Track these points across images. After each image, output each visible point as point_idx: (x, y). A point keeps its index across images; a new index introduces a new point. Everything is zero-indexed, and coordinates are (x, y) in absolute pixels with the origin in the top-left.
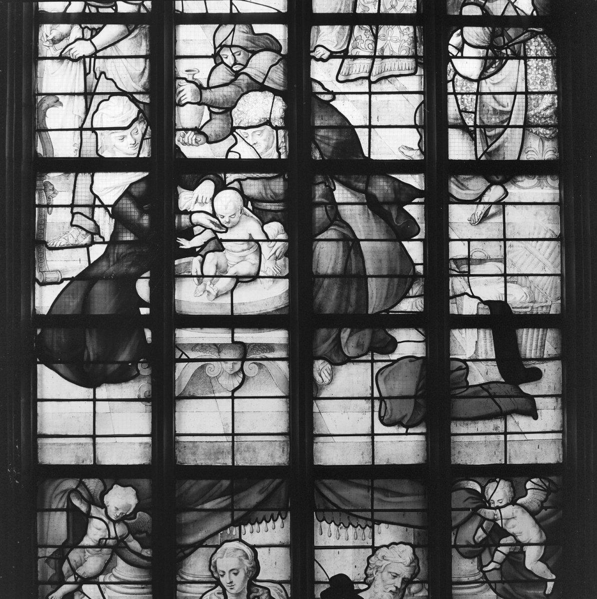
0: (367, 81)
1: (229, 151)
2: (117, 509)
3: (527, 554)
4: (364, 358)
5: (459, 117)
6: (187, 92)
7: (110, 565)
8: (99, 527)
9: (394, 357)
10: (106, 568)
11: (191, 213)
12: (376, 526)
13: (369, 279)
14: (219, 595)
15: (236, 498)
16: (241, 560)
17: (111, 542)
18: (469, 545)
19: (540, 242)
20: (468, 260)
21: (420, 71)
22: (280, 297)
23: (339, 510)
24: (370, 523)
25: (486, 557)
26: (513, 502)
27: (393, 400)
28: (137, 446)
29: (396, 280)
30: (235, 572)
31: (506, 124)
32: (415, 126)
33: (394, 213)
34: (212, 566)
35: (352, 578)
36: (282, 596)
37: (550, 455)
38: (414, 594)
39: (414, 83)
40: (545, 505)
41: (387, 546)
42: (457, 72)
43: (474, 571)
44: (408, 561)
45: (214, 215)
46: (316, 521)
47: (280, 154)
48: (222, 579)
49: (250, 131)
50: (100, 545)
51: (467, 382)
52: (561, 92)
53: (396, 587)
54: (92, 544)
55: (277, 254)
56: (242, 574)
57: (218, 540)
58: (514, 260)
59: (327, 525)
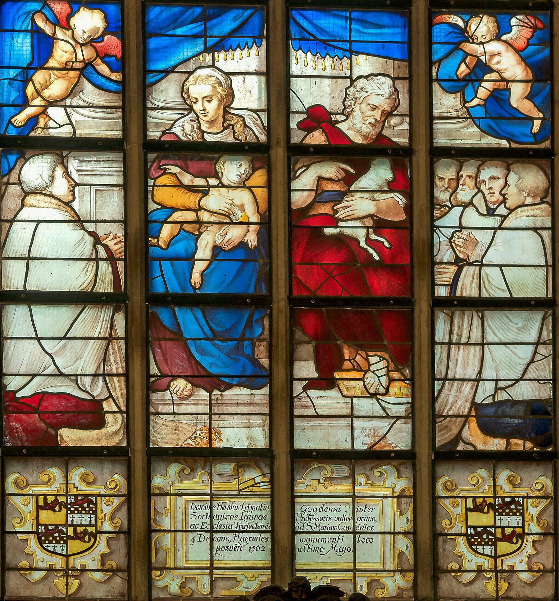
2: (84, 32)
8: (65, 49)
14: (192, 123)
15: (208, 24)
16: (214, 87)
17: (78, 65)
23: (315, 38)
25: (469, 91)
30: (209, 99)
34: (183, 91)
35: (329, 109)
36: (257, 125)
41: (366, 77)
48: (195, 107)
53: (376, 119)
54: (58, 66)
56: (215, 103)
57: (190, 66)
59: (303, 55)
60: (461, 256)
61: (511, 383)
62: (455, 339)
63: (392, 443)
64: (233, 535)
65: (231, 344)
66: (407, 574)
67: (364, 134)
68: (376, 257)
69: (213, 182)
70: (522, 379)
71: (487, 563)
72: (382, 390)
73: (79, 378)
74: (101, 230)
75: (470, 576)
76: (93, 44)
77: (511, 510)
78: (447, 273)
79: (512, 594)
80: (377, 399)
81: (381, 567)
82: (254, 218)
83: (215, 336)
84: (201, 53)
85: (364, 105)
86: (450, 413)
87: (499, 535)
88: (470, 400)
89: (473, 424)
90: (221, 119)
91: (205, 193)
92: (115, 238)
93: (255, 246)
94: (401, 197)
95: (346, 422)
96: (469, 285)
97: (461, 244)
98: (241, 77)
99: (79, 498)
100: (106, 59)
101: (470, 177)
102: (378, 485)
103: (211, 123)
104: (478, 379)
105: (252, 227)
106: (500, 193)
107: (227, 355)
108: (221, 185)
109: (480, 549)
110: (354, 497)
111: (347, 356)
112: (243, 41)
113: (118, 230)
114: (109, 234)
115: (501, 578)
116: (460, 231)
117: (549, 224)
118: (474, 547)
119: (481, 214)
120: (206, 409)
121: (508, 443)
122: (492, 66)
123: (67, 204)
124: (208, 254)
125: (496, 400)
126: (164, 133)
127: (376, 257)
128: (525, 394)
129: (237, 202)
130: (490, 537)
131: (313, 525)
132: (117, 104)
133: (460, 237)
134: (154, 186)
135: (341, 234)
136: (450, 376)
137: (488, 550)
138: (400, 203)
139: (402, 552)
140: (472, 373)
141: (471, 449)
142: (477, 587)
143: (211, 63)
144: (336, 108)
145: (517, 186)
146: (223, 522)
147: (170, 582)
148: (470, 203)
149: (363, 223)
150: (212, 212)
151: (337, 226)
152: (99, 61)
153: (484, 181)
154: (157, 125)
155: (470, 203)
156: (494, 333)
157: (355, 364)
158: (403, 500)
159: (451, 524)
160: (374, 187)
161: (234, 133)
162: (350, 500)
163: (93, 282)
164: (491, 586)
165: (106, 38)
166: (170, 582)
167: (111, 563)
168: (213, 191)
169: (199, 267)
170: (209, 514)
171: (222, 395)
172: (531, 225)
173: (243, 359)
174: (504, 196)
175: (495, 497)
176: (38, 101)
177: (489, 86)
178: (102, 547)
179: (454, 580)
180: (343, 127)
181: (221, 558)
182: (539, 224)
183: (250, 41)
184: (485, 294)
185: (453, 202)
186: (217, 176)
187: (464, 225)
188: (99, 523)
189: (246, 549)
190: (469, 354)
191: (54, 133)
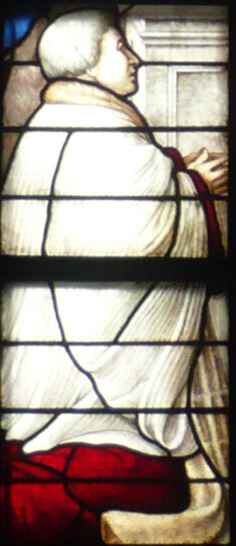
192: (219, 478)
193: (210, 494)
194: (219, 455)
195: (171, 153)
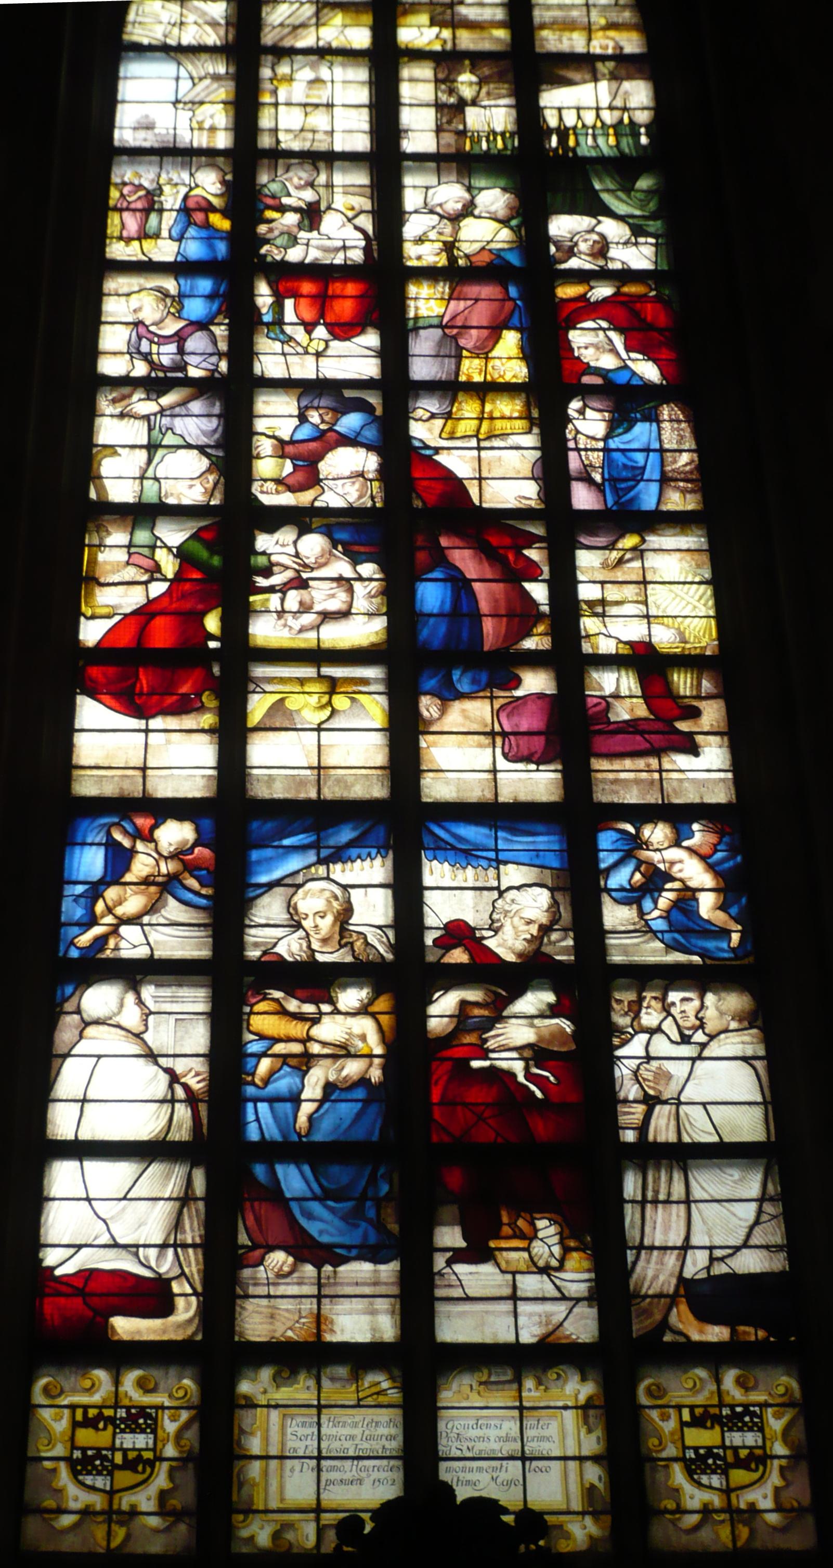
0: (475, 439)
1: (315, 499)
2: (170, 844)
3: (700, 901)
4: (481, 694)
5: (583, 471)
6: (264, 446)
7: (159, 904)
8: (146, 862)
9: (519, 693)
10: (152, 909)
11: (270, 555)
12: (501, 867)
13: (484, 619)
14: (301, 941)
15: (322, 834)
16: (329, 902)
17: (160, 879)
18: (622, 889)
19: (687, 586)
20: (603, 602)
21: (536, 430)
22: (377, 633)
23: (454, 848)
24: (494, 864)
25: (647, 904)
26: (677, 843)
27: (518, 737)
28: (198, 780)
29: (516, 620)
30: (322, 914)
31: (639, 478)
32: (533, 478)
33: (511, 557)
34: (291, 907)
35: (472, 924)
36: (383, 942)
37: (720, 795)
38: (555, 943)
39: (530, 440)
40: (719, 848)
41: (518, 888)
42: (578, 432)
43: (633, 919)
44: (546, 906)
45: (297, 555)
46: (424, 861)
47: (374, 502)
48: (304, 923)
49: (340, 482)
50: (146, 882)
51: (608, 719)
52: (701, 449)
53: (532, 935)
54: (135, 880)
55: (373, 593)
56: (330, 919)
57: (300, 879)
58: (658, 603)
59: (440, 865)
60: (651, 1092)
61: (730, 1251)
62: (650, 1195)
63: (572, 1334)
64: (349, 1462)
65: (349, 1205)
66: (602, 1517)
67: (517, 951)
68: (539, 1094)
69: (326, 1008)
70: (745, 1245)
71: (717, 1501)
72: (554, 1263)
73: (141, 1250)
74: (180, 1066)
75: (694, 1519)
76: (181, 857)
77: (745, 1424)
78: (633, 1114)
79: (757, 1544)
80: (549, 1276)
81: (564, 1507)
82: (378, 1050)
83: (325, 1196)
84: (314, 865)
85: (516, 919)
86: (651, 1292)
87: (730, 1458)
88: (677, 1274)
89: (684, 1307)
90: (337, 937)
91: (315, 1020)
92: (197, 1074)
93: (380, 1083)
94: (568, 1023)
95: (507, 1306)
96: (664, 1128)
97: (650, 1078)
98: (362, 890)
99: (133, 1411)
100: (196, 873)
101: (655, 998)
102: (554, 1391)
103: (325, 941)
104: (686, 1247)
105: (377, 1061)
106: (697, 1017)
107: (343, 1218)
108: (337, 1012)
109: (705, 1479)
110: (521, 1408)
111: (505, 1219)
112: (364, 852)
113: (199, 1065)
114: (190, 1070)
115: (739, 1522)
116: (648, 1063)
117: (761, 1052)
118: (696, 1477)
119: (672, 1042)
120: (313, 1290)
121: (733, 1332)
122: (673, 874)
123: (138, 1036)
124: (318, 1093)
125: (712, 1274)
126: (265, 953)
127: (539, 1094)
128: (752, 1266)
129: (357, 1031)
130: (718, 1462)
131: (464, 1448)
132: (207, 921)
133: (647, 1070)
134: (251, 1013)
135: (492, 1067)
136: (647, 1242)
137: (716, 1481)
138: (568, 1030)
139: (592, 1486)
140: (676, 1239)
141: (682, 1339)
142: (705, 1535)
143: (325, 875)
144: (481, 923)
145: (717, 1009)
146: (336, 1445)
147: (258, 1530)
148: (658, 1030)
149: (520, 1054)
150: (324, 1044)
151: (486, 1058)
152: (187, 875)
153: (673, 1004)
154: (256, 945)
155: (658, 1030)
156: (703, 1188)
157: (517, 1230)
158: (592, 1412)
159: (661, 1443)
160: (532, 1011)
161: (353, 951)
162: (516, 1413)
163: (166, 1128)
164: (725, 1533)
165: (197, 850)
166: (258, 1530)
167: (175, 1503)
168: (326, 1020)
169: (307, 1109)
170: (316, 1433)
171: (335, 1272)
172: (740, 1054)
173: (364, 1225)
174: (701, 1020)
175: (721, 1405)
176: (109, 919)
177: (671, 896)
178: (161, 1480)
179: (671, 1526)
180: (491, 943)
181: (332, 1496)
182: (749, 1052)
183: (374, 851)
184: (686, 1139)
185: (636, 1027)
186: (332, 1001)
187: (652, 1054)
188: (160, 1445)
189: (368, 1483)
190: (670, 1214)
191: (125, 954)
192: (195, 1293)
193: (189, 1304)
194: (196, 1277)
195: (169, 1071)
